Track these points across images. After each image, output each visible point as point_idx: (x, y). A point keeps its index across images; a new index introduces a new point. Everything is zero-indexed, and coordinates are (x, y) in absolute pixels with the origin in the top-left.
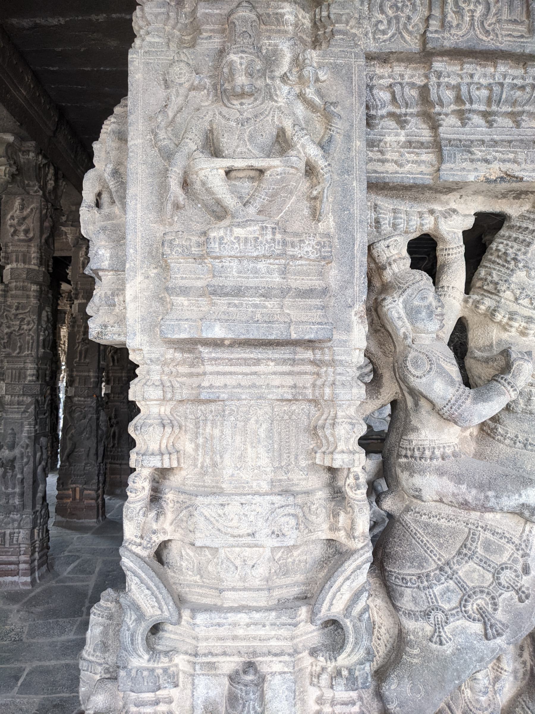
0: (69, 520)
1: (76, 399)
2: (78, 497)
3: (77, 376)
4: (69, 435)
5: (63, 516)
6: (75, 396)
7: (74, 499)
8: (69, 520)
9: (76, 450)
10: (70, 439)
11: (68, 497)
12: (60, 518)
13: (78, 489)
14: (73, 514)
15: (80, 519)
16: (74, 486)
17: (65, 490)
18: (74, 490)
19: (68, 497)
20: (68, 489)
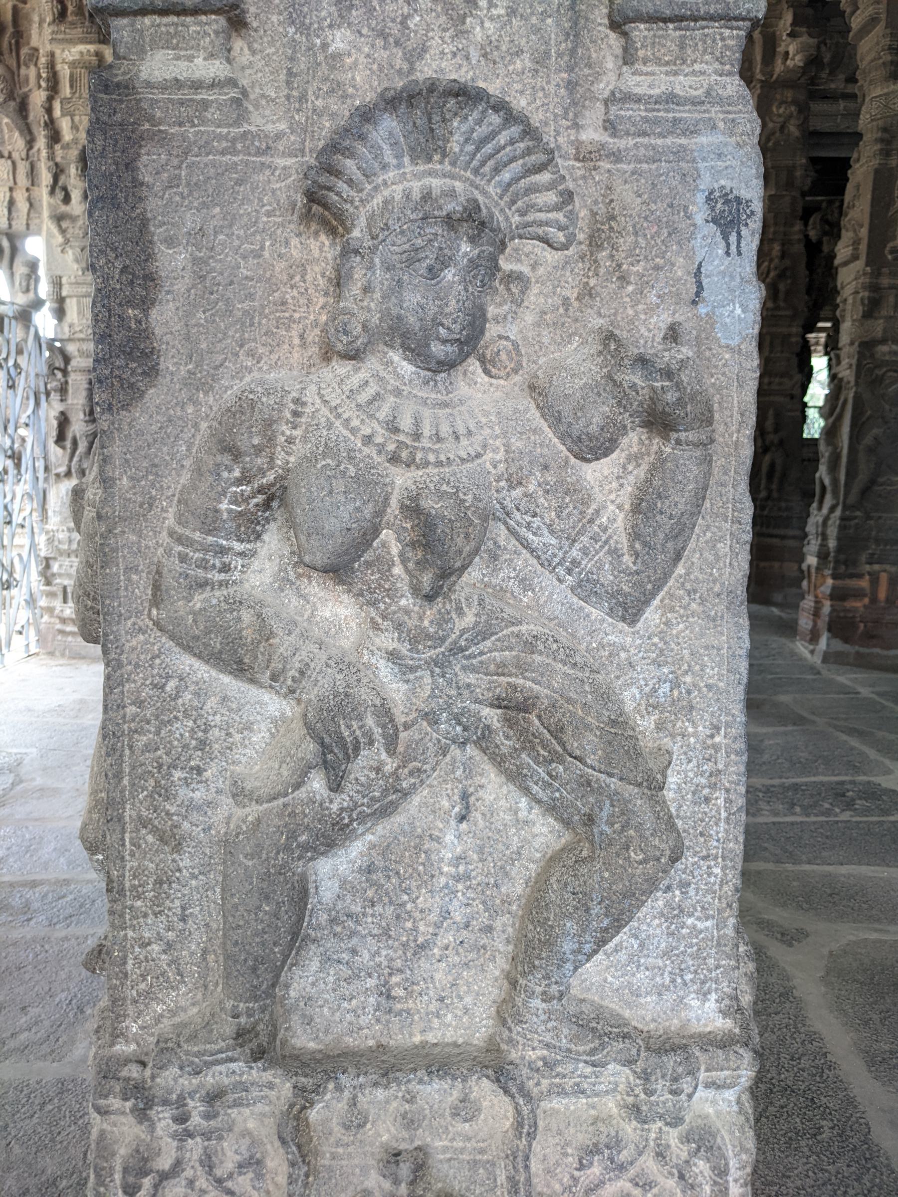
0: (862, 650)
1: (884, 348)
2: (882, 594)
3: (891, 287)
4: (868, 440)
5: (846, 640)
6: (883, 341)
7: (874, 600)
8: (862, 650)
9: (881, 480)
10: (870, 450)
11: (858, 594)
12: (839, 645)
13: (884, 577)
14: (873, 637)
15: (889, 648)
16: (876, 567)
17: (852, 576)
18: (875, 580)
19: (858, 594)
20: (860, 576)
